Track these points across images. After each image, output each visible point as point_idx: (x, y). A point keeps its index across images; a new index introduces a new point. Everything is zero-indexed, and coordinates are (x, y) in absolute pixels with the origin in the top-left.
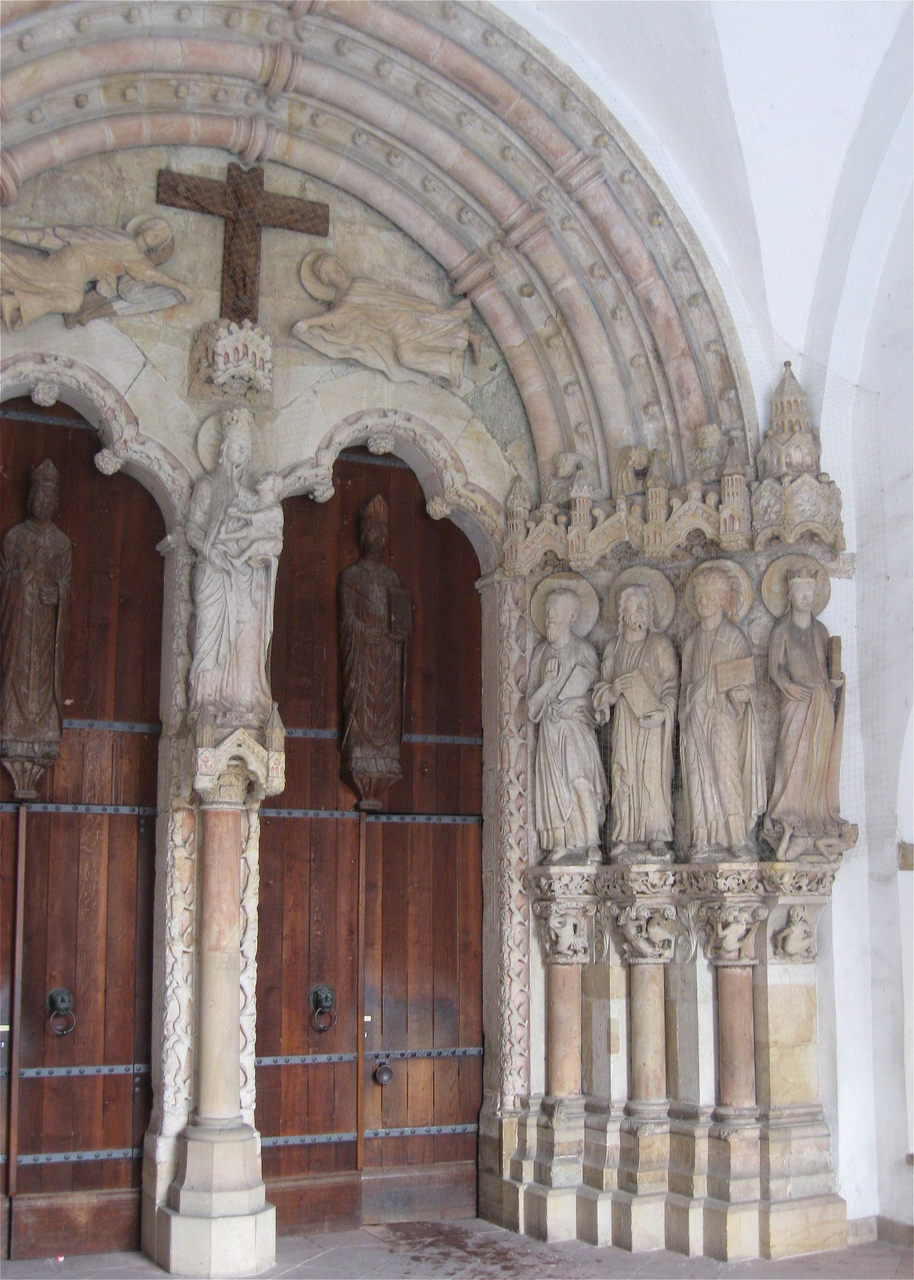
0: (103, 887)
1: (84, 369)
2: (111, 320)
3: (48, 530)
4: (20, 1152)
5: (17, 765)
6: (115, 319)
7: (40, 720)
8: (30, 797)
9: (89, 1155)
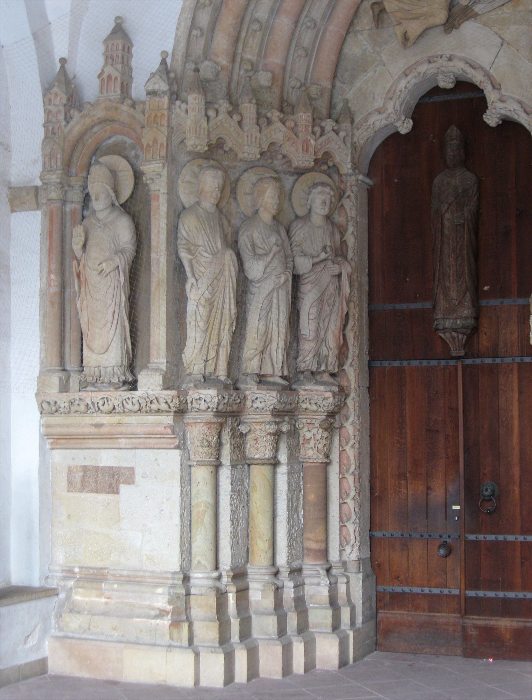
0: (516, 413)
1: (461, 59)
2: (476, 19)
3: (458, 174)
4: (466, 589)
5: (448, 335)
6: (478, 17)
7: (459, 304)
8: (460, 355)
9: (511, 595)
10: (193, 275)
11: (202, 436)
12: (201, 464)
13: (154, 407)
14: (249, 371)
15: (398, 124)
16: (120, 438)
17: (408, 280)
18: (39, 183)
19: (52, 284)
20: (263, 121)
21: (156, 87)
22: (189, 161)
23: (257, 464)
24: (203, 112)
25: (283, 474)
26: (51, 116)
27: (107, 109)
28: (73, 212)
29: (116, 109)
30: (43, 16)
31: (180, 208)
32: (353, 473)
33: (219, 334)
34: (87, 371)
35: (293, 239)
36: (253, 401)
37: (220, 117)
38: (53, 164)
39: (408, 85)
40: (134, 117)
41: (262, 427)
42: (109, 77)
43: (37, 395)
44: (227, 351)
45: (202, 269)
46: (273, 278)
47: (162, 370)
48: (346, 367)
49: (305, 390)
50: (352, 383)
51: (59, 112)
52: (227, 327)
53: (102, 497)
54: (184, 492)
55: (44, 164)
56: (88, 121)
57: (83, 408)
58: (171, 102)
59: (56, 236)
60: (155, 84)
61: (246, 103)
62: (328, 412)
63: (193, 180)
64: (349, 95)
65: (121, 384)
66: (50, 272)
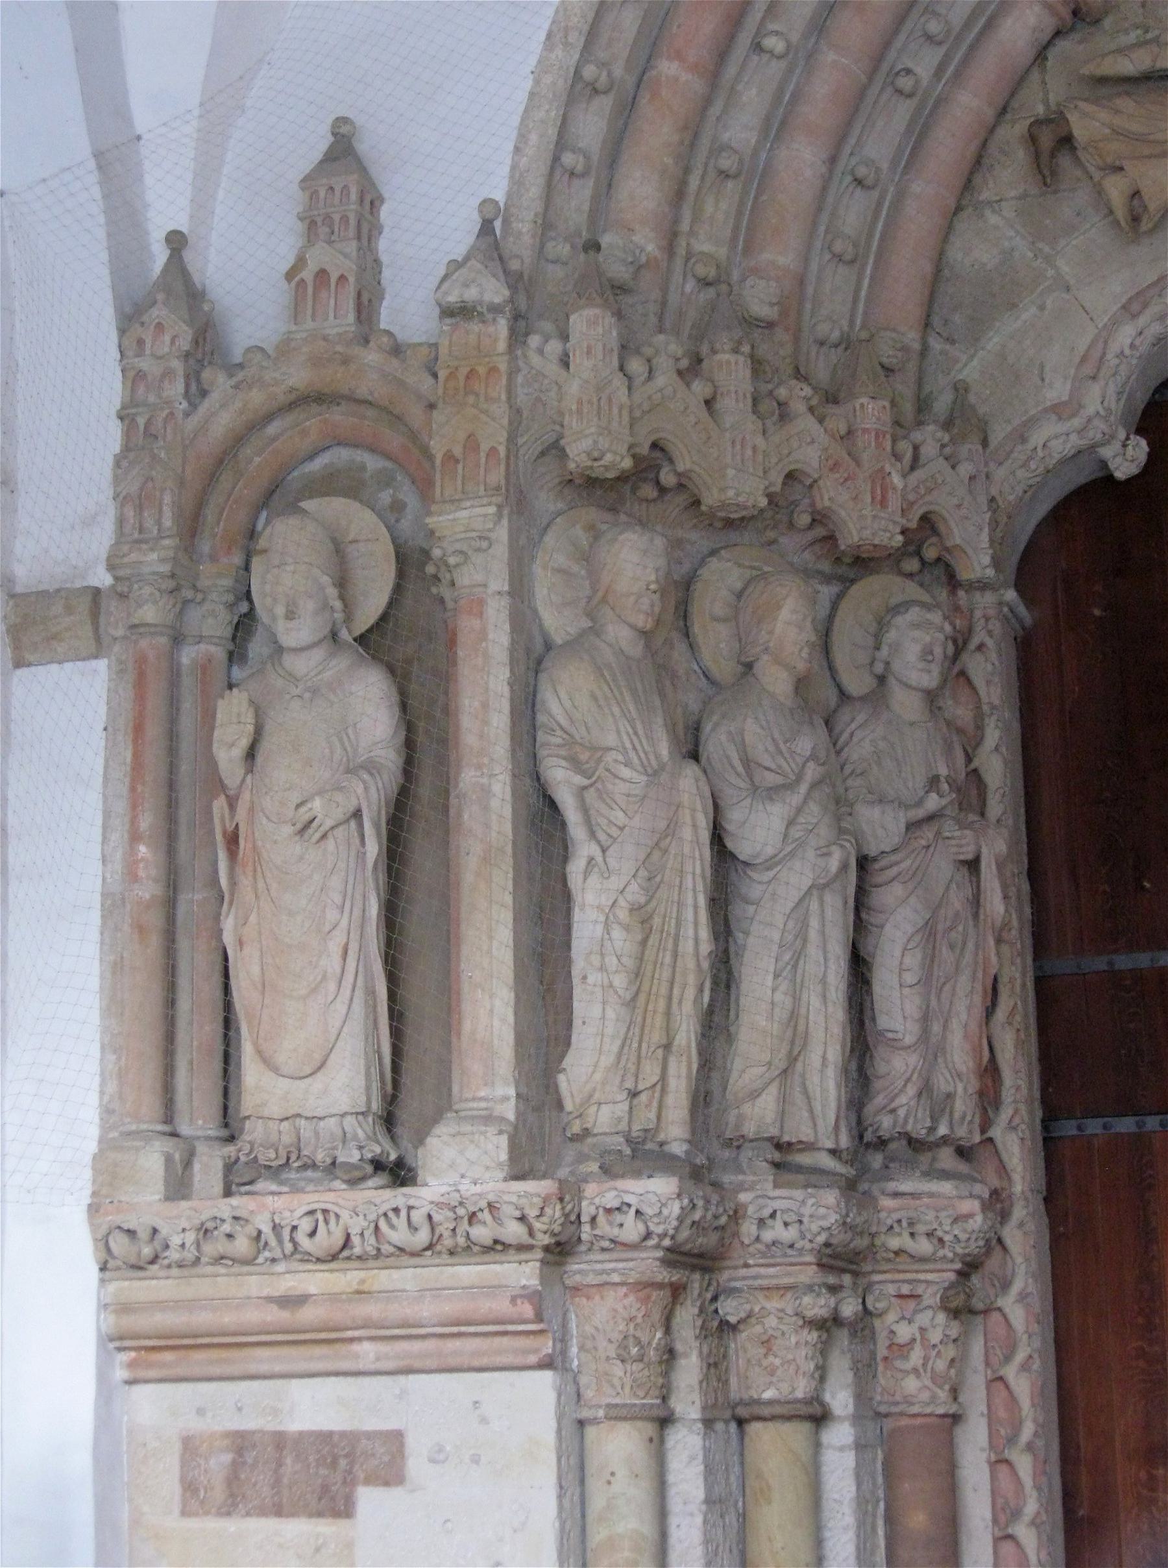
10: (592, 834)
11: (622, 1327)
12: (618, 1414)
13: (482, 1233)
14: (750, 1129)
15: (1106, 452)
16: (359, 1339)
17: (1147, 885)
18: (102, 578)
19: (142, 873)
20: (766, 405)
21: (471, 294)
22: (559, 513)
23: (773, 1418)
24: (615, 363)
25: (842, 1449)
26: (141, 390)
27: (316, 362)
28: (204, 668)
29: (346, 361)
30: (123, 114)
31: (539, 647)
32: (1030, 1447)
33: (668, 1013)
34: (254, 1132)
35: (844, 755)
36: (761, 1222)
37: (660, 381)
38: (149, 523)
39: (1137, 342)
40: (401, 383)
41: (788, 1304)
42: (322, 275)
43: (94, 1209)
45: (619, 817)
46: (811, 854)
47: (503, 1119)
48: (996, 1132)
49: (896, 1195)
50: (1017, 1177)
51: (168, 374)
52: (690, 993)
53: (297, 1528)
54: (566, 1503)
55: (121, 522)
56: (257, 398)
57: (242, 1245)
58: (517, 337)
59: (154, 731)
60: (466, 285)
61: (724, 351)
62: (963, 1258)
63: (575, 568)
64: (970, 371)
65: (369, 1169)
66: (135, 837)
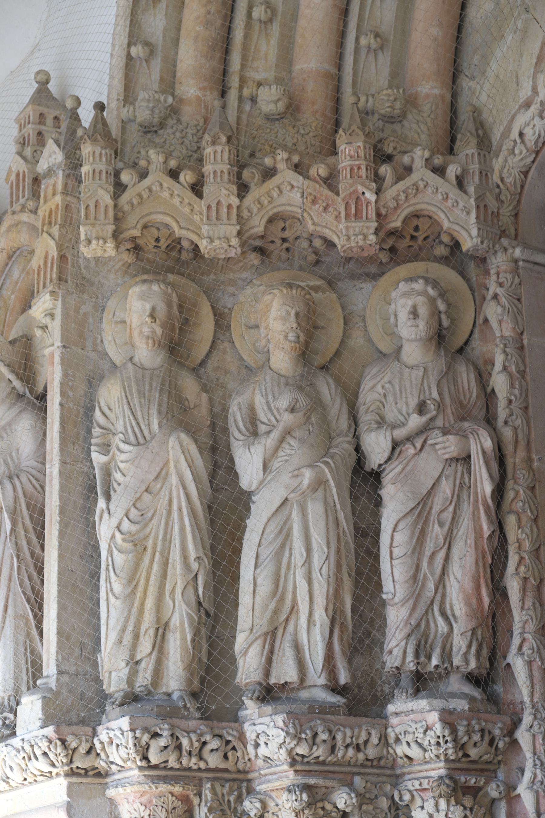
44: (184, 639)
